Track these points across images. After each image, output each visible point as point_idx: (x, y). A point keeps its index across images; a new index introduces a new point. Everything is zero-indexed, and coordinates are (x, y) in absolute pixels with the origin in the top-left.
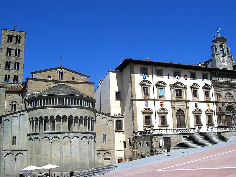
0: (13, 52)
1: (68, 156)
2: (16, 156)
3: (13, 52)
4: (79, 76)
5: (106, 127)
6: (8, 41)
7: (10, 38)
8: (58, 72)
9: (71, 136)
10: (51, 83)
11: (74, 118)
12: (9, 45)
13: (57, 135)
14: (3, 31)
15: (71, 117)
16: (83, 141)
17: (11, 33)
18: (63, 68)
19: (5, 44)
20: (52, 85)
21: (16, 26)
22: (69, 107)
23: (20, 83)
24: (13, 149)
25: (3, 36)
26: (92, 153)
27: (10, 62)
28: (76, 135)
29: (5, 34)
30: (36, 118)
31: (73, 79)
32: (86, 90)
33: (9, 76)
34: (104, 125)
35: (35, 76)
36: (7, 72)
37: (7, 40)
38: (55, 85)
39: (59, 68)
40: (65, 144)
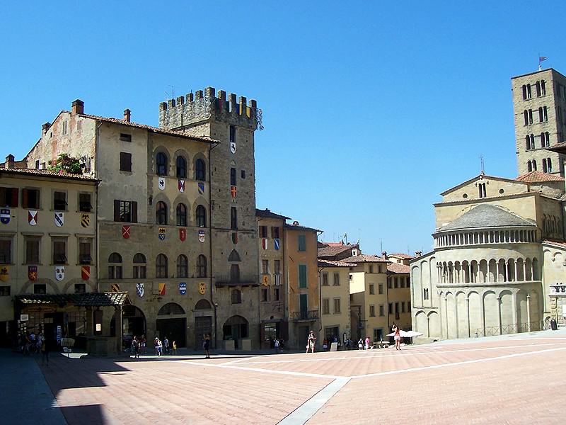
0: (536, 115)
1: (463, 321)
2: (428, 315)
3: (536, 115)
4: (512, 184)
5: (563, 270)
6: (525, 98)
7: (527, 89)
8: (478, 185)
9: (467, 290)
10: (467, 206)
11: (461, 264)
12: (527, 105)
13: (450, 290)
14: (513, 82)
15: (465, 262)
16: (487, 299)
17: (526, 80)
18: (484, 177)
19: (520, 105)
20: (469, 208)
21: (541, 59)
22: (462, 248)
23: (555, 171)
24: (425, 305)
25: (515, 90)
26: (512, 317)
27: (532, 135)
28: (473, 289)
29: (517, 86)
30: (445, 263)
31: (502, 191)
32: (523, 208)
33: (535, 162)
34: (559, 267)
35: (447, 199)
36: (530, 156)
37: (521, 97)
38: (473, 207)
39: (478, 178)
40: (460, 303)
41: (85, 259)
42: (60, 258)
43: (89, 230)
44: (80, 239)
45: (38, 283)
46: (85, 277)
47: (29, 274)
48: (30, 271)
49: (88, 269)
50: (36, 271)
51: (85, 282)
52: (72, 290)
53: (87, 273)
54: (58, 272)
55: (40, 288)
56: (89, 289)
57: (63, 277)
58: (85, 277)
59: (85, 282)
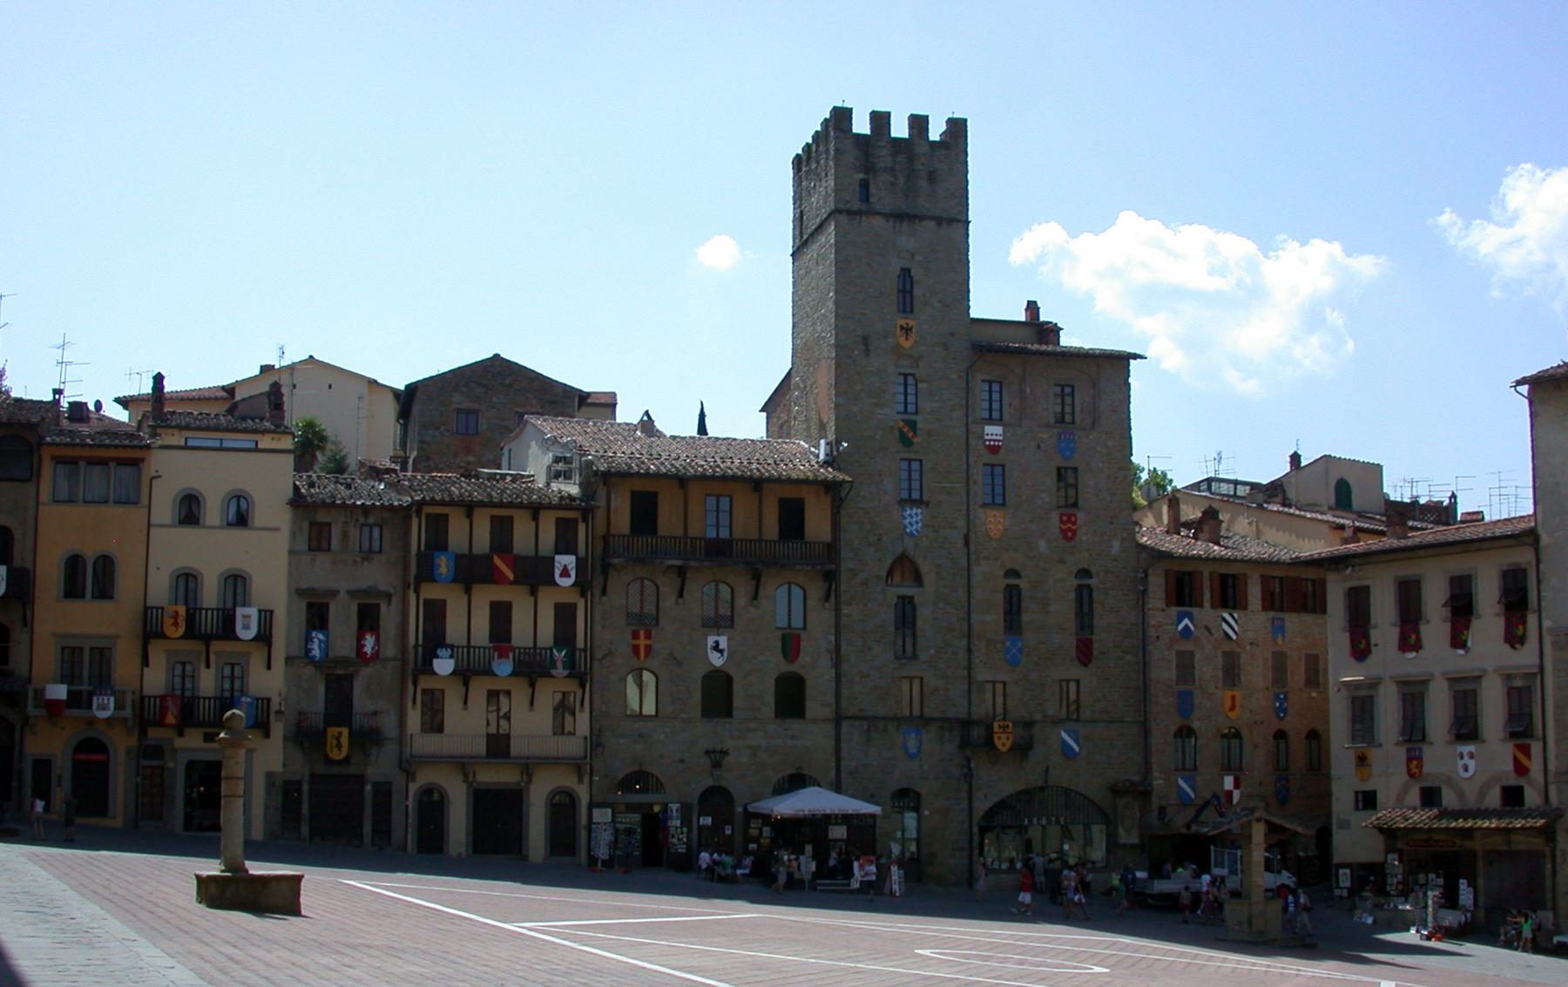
41: (1521, 729)
42: (1466, 729)
43: (1525, 657)
44: (1508, 677)
45: (1429, 784)
46: (1521, 770)
47: (1408, 766)
48: (1410, 760)
49: (1526, 750)
50: (1420, 759)
51: (1521, 782)
52: (1494, 799)
53: (1522, 758)
54: (1462, 758)
55: (1430, 797)
56: (1532, 798)
57: (1471, 770)
58: (1521, 770)
59: (1521, 782)
